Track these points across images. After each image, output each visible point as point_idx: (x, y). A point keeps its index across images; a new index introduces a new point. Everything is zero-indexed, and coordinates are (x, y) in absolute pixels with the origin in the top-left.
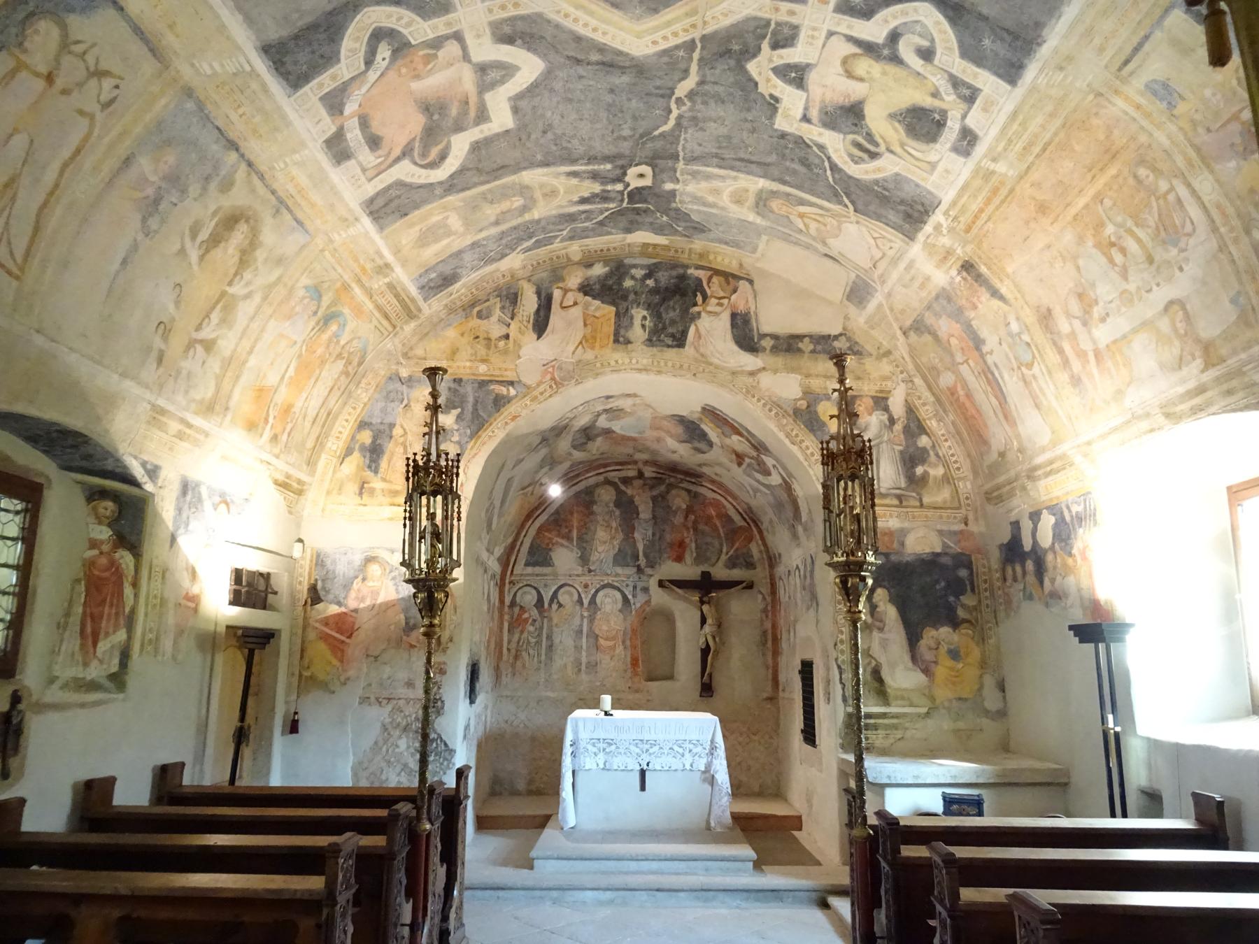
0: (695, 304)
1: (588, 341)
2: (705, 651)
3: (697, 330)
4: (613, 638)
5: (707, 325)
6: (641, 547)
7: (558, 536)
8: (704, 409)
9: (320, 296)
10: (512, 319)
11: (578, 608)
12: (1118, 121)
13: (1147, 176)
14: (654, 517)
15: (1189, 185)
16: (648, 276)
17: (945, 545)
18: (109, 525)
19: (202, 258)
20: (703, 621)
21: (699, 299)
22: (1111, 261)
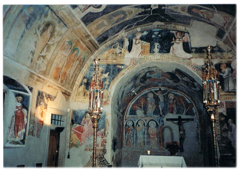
0: (173, 41)
1: (142, 53)
3: (173, 47)
5: (176, 46)
7: (138, 107)
8: (176, 70)
9: (72, 44)
10: (122, 48)
11: (144, 126)
14: (164, 101)
16: (159, 34)
18: (21, 103)
19: (41, 35)
21: (174, 39)
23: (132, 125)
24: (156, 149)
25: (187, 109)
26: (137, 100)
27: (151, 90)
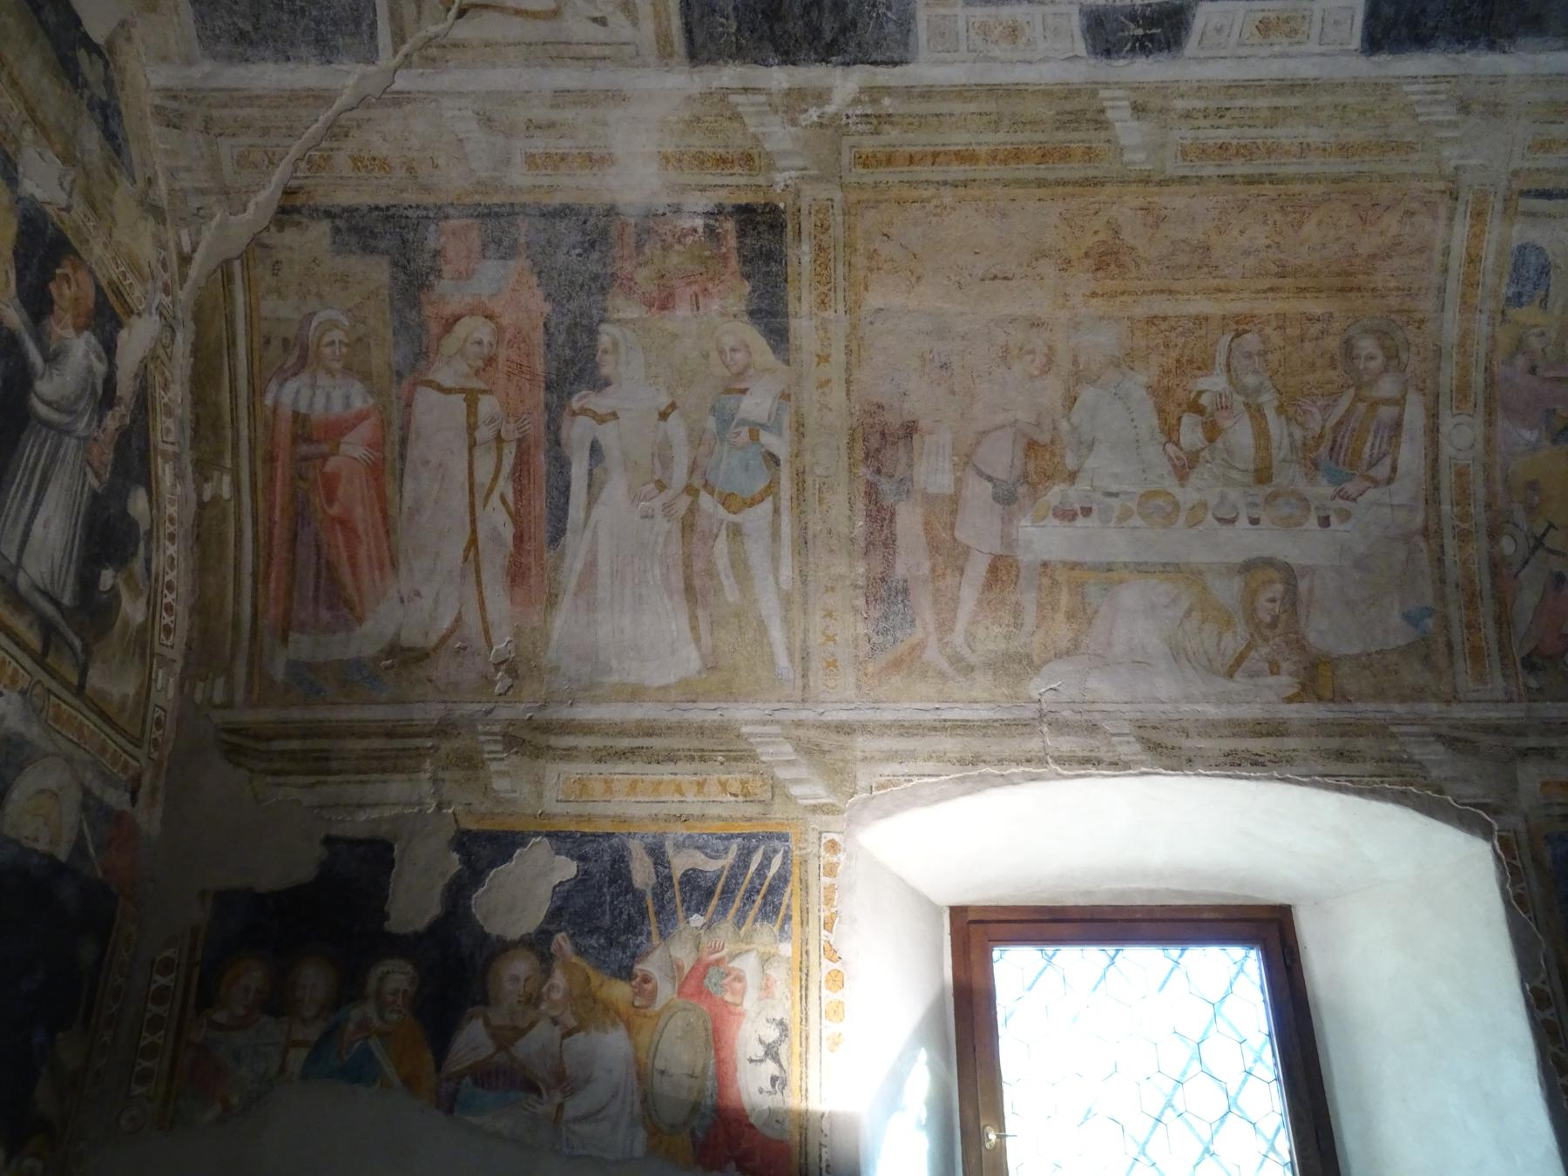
12: (1421, 251)
13: (1371, 358)
15: (1433, 416)
17: (79, 848)
22: (1170, 432)
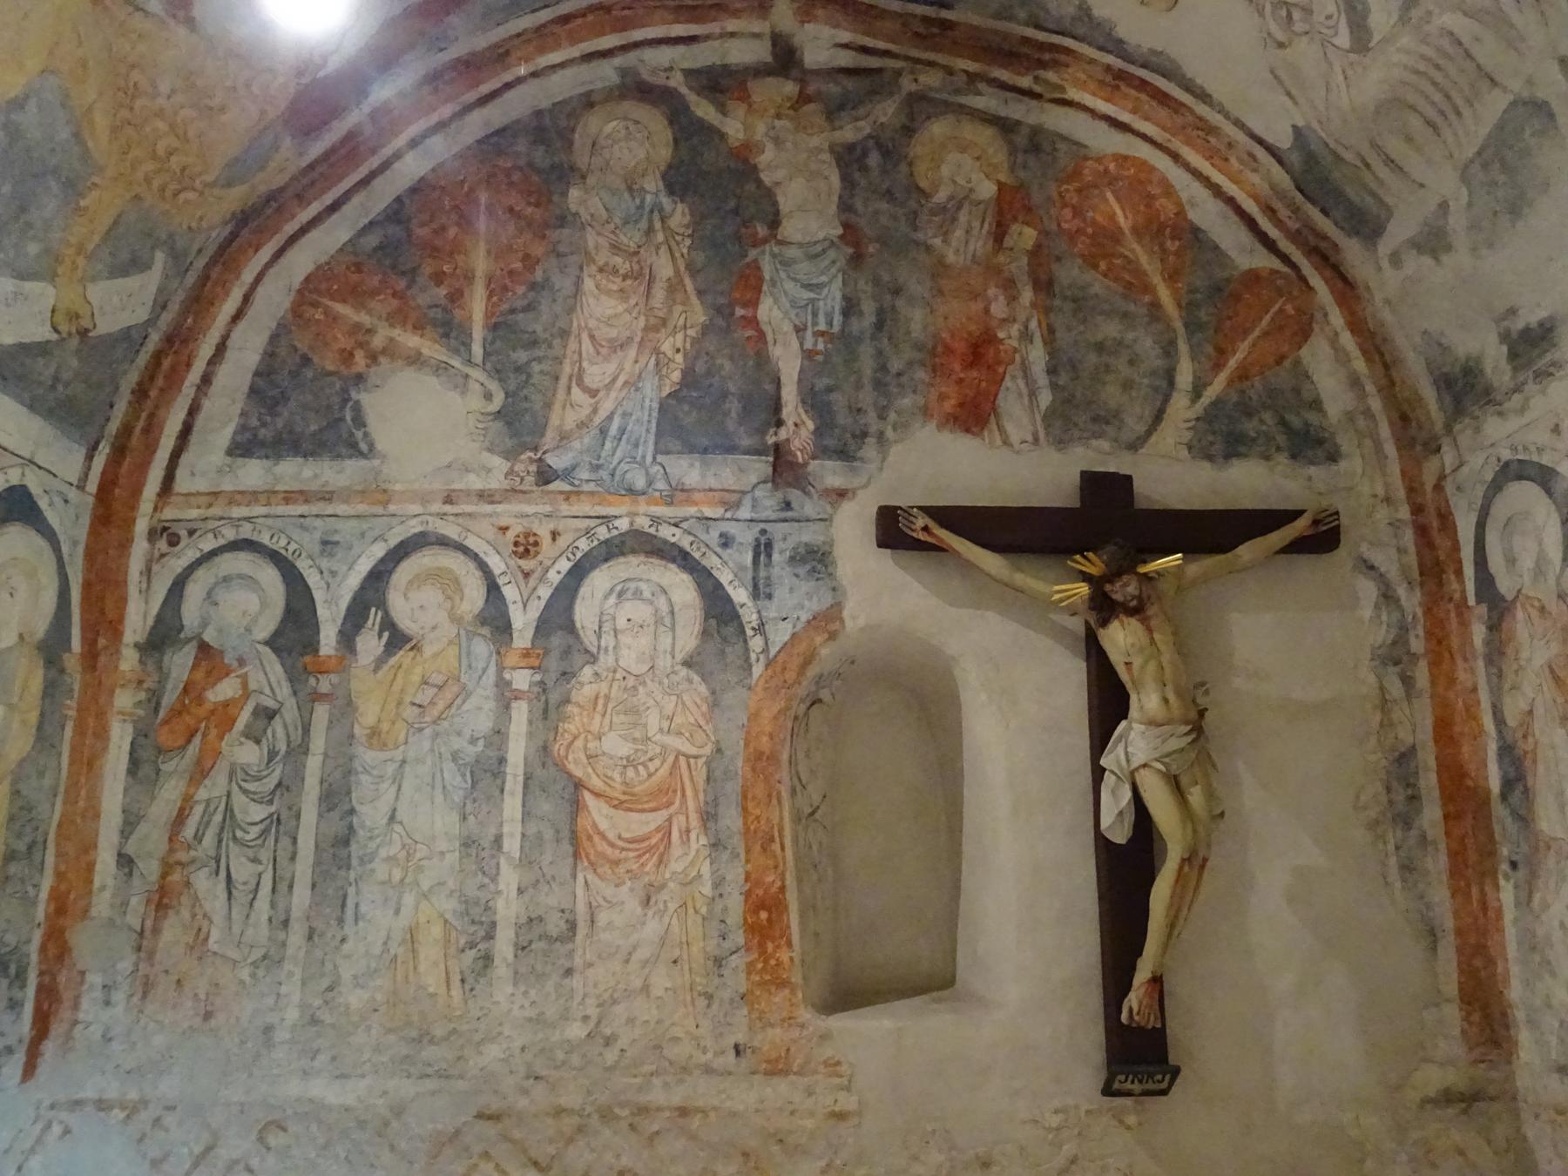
2: (1126, 869)
4: (663, 796)
6: (788, 362)
7: (398, 317)
11: (482, 648)
14: (851, 234)
20: (1108, 702)
23: (268, 624)
24: (676, 1052)
25: (1218, 367)
26: (396, 213)
27: (630, 59)
